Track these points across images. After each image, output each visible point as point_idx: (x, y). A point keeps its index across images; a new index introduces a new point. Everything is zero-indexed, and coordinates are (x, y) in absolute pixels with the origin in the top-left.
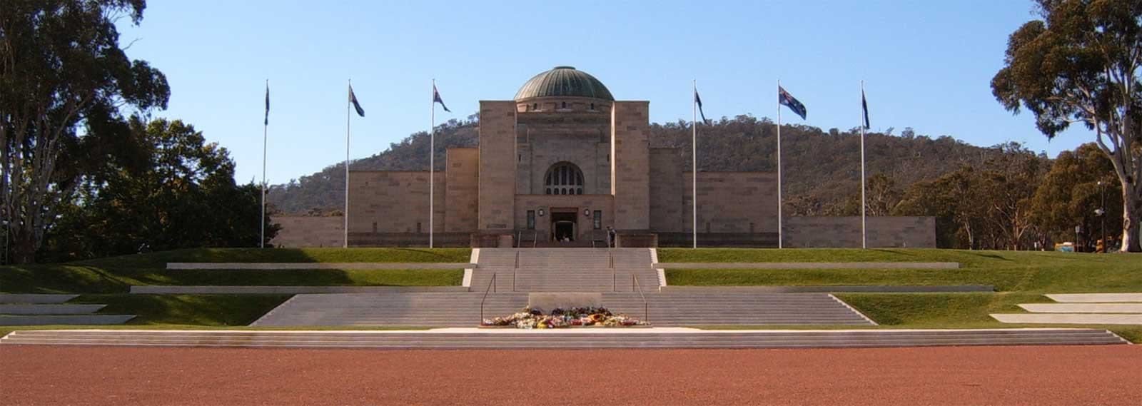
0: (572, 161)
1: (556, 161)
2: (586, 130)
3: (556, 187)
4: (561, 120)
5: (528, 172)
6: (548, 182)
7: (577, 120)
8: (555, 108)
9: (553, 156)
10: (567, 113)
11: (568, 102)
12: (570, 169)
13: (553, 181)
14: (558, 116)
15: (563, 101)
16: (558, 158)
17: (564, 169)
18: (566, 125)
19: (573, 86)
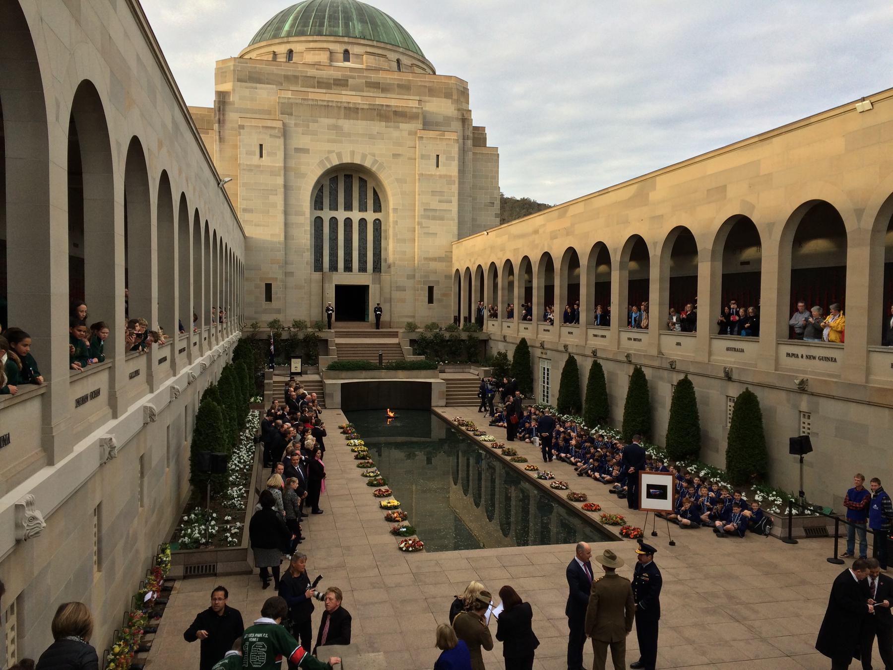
0: (367, 164)
1: (336, 162)
2: (393, 103)
3: (334, 214)
4: (341, 83)
5: (280, 181)
6: (318, 204)
7: (375, 86)
8: (331, 60)
9: (330, 152)
10: (352, 69)
11: (354, 50)
12: (361, 179)
13: (326, 202)
14: (338, 75)
15: (344, 47)
16: (339, 155)
17: (348, 178)
18: (354, 93)
19: (362, 21)
